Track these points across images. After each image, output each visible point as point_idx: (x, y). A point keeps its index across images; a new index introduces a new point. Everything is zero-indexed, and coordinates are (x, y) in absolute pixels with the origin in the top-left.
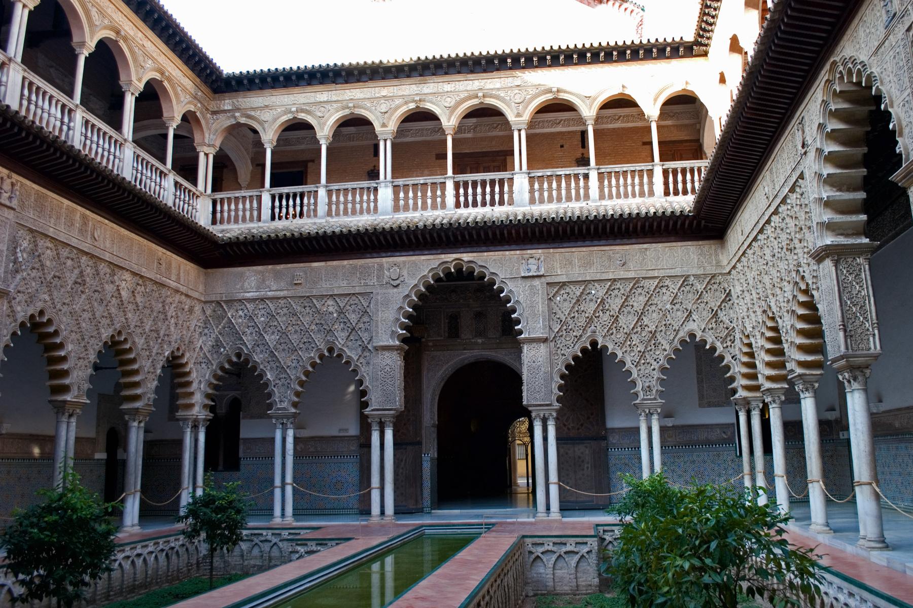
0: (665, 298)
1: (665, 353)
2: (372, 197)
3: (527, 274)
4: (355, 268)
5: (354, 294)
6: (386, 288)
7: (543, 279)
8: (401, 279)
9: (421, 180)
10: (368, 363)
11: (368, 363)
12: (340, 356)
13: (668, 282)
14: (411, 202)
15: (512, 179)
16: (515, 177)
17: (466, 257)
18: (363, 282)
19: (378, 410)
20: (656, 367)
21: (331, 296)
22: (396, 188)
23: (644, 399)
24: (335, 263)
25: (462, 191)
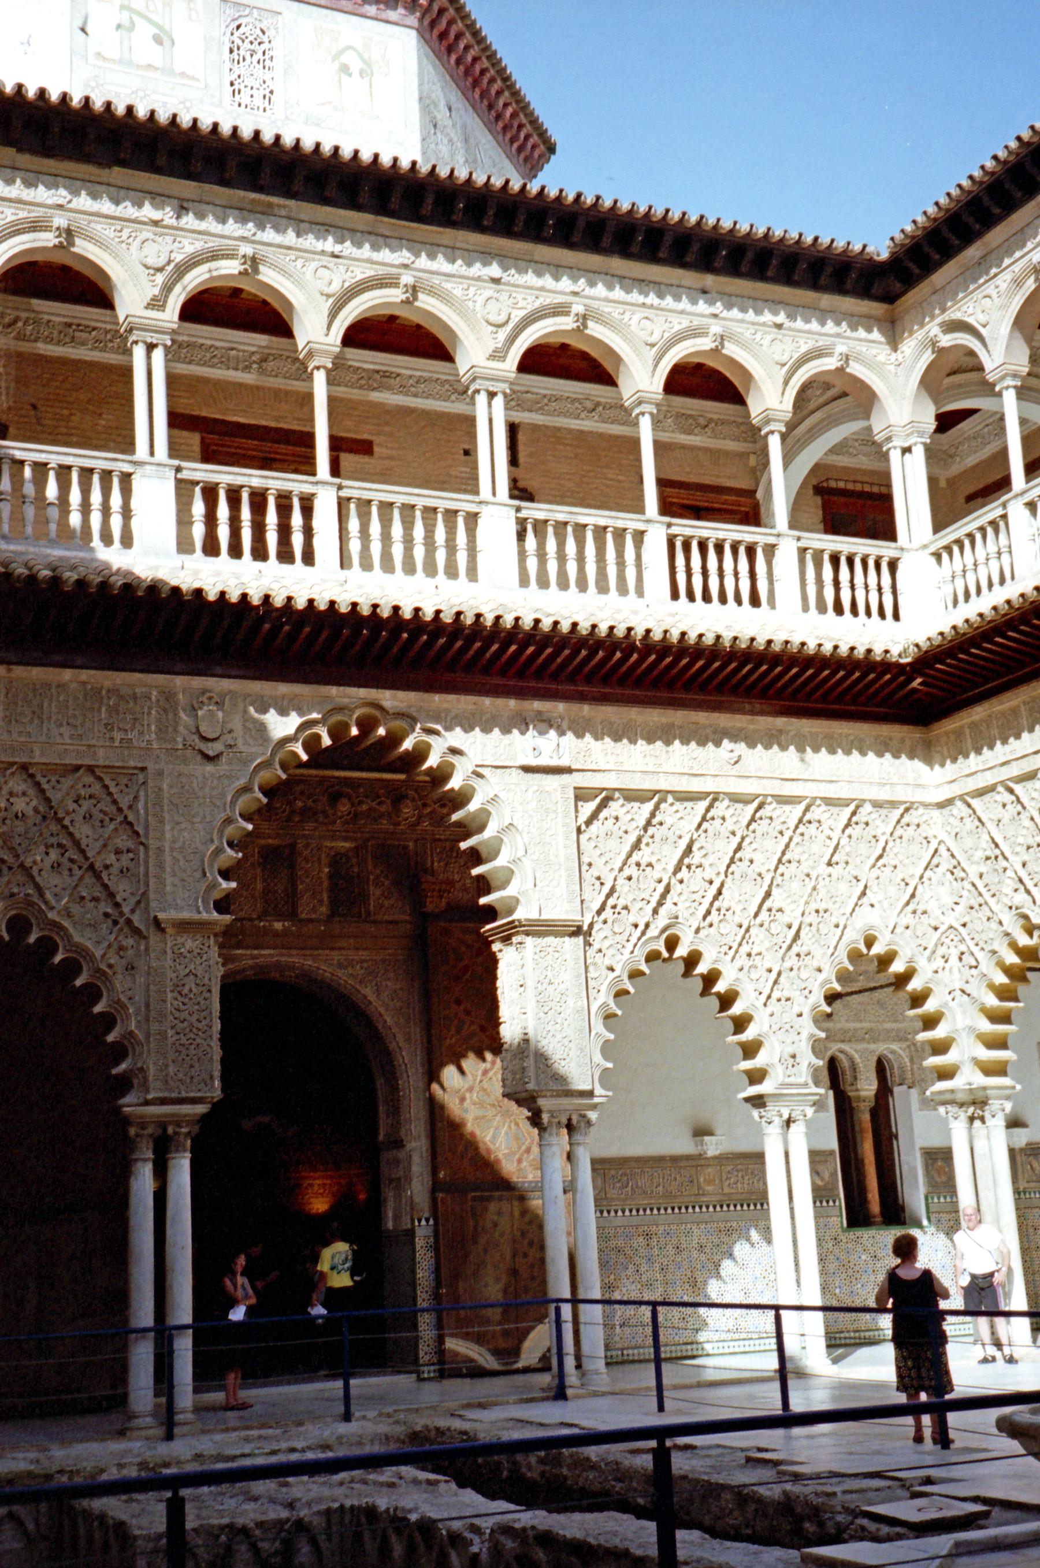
0: (815, 848)
1: (821, 977)
2: (116, 500)
3: (533, 762)
4: (96, 693)
5: (91, 769)
6: (185, 760)
7: (565, 777)
8: (228, 739)
9: (253, 478)
10: (130, 968)
11: (130, 968)
12: (47, 946)
13: (818, 812)
14: (223, 533)
15: (476, 515)
16: (485, 512)
17: (390, 699)
18: (118, 736)
19: (163, 1101)
20: (806, 1011)
21: (24, 767)
22: (184, 488)
23: (784, 1085)
24: (37, 673)
25: (354, 525)
